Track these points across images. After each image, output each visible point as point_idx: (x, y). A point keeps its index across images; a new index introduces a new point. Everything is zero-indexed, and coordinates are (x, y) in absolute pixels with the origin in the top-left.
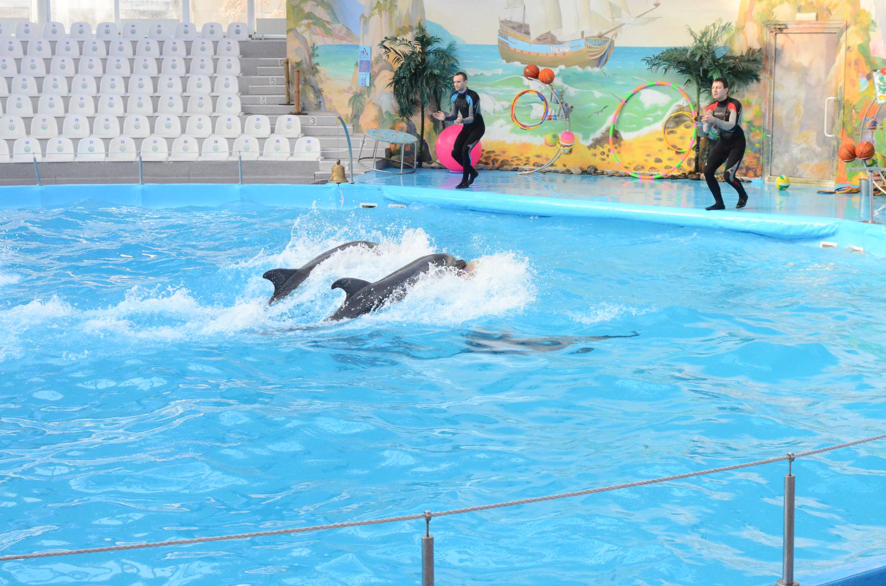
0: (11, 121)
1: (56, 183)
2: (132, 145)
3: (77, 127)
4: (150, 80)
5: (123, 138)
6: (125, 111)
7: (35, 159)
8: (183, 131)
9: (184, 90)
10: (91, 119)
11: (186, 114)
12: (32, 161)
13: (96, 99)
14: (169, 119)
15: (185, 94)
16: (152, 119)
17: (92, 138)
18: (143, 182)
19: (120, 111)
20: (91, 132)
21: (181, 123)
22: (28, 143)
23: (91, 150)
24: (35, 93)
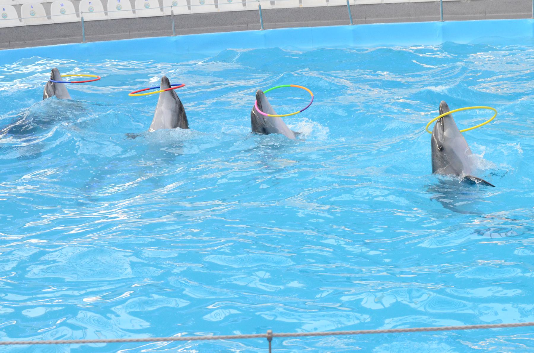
1: (366, 23)
18: (443, 20)
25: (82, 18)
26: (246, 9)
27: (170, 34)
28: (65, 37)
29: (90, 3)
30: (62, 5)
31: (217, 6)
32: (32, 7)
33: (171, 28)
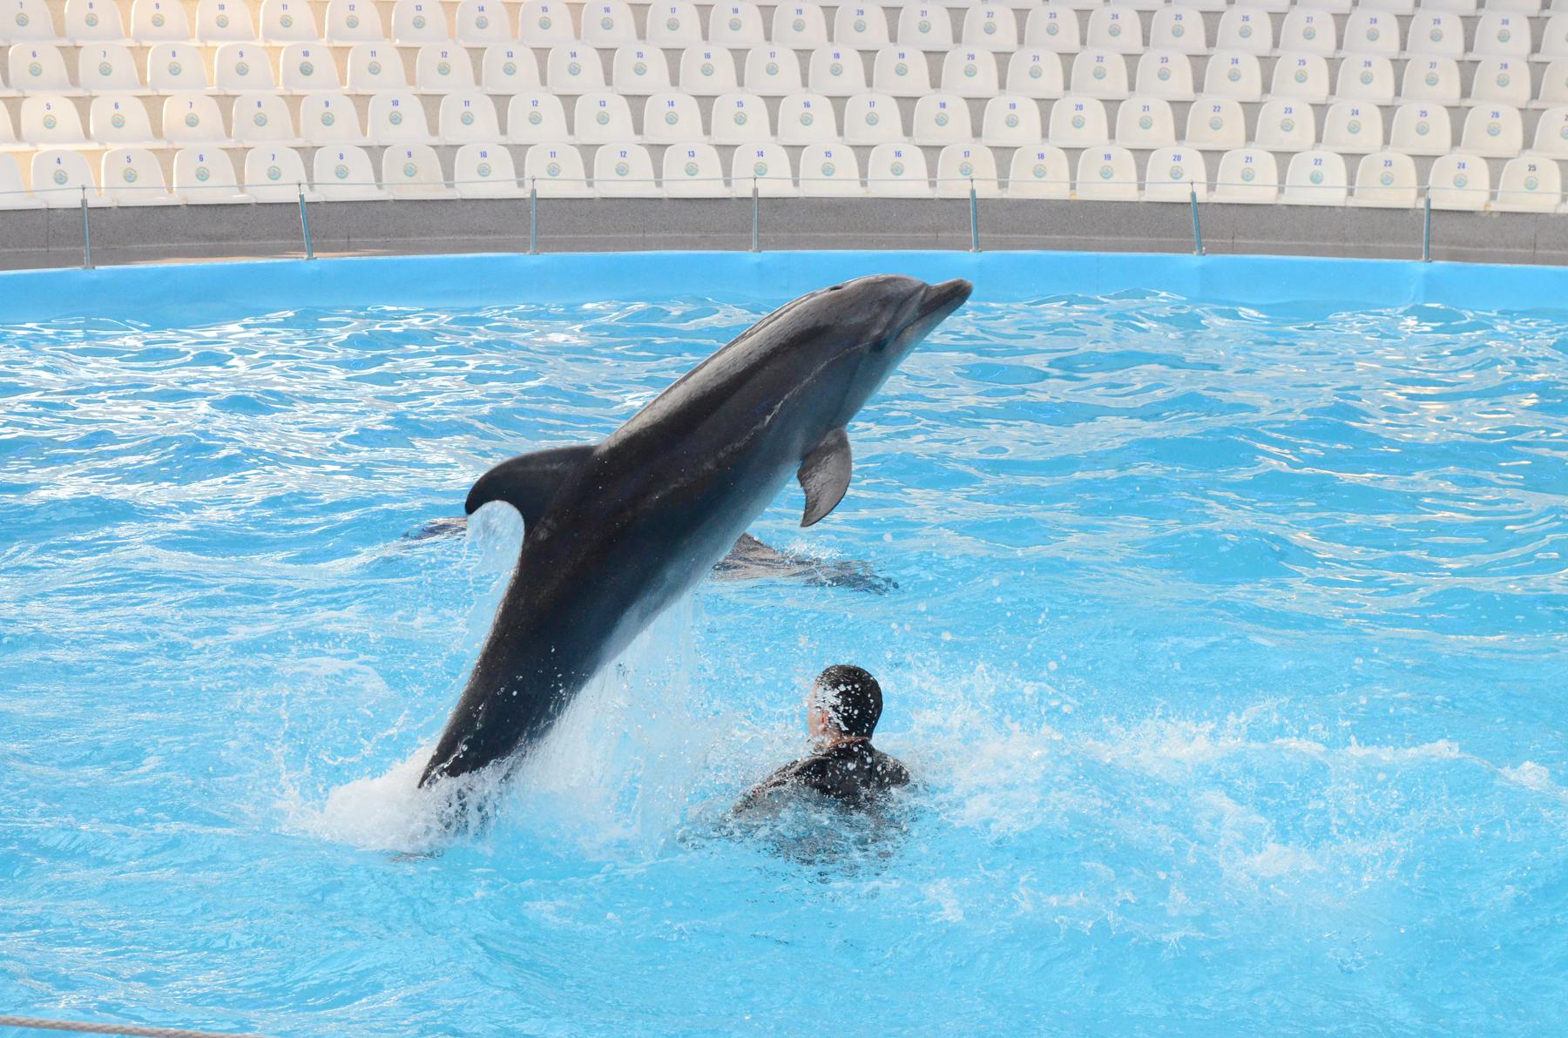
0: (1146, 108)
1: (1233, 249)
2: (1408, 172)
3: (1287, 127)
4: (1459, 21)
5: (1389, 153)
6: (1398, 93)
7: (1193, 195)
8: (1528, 143)
9: (1536, 48)
10: (1320, 109)
11: (1535, 105)
12: (1188, 199)
13: (1334, 64)
14: (1496, 115)
15: (1537, 58)
16: (1457, 114)
17: (1318, 153)
18: (1430, 257)
19: (1387, 96)
20: (1319, 139)
21: (1524, 125)
22: (1178, 158)
23: (1316, 179)
24: (1200, 47)
25: (534, 192)
26: (937, 196)
27: (744, 244)
28: (488, 233)
29: (553, 154)
30: (484, 155)
31: (864, 184)
32: (410, 154)
33: (746, 229)
